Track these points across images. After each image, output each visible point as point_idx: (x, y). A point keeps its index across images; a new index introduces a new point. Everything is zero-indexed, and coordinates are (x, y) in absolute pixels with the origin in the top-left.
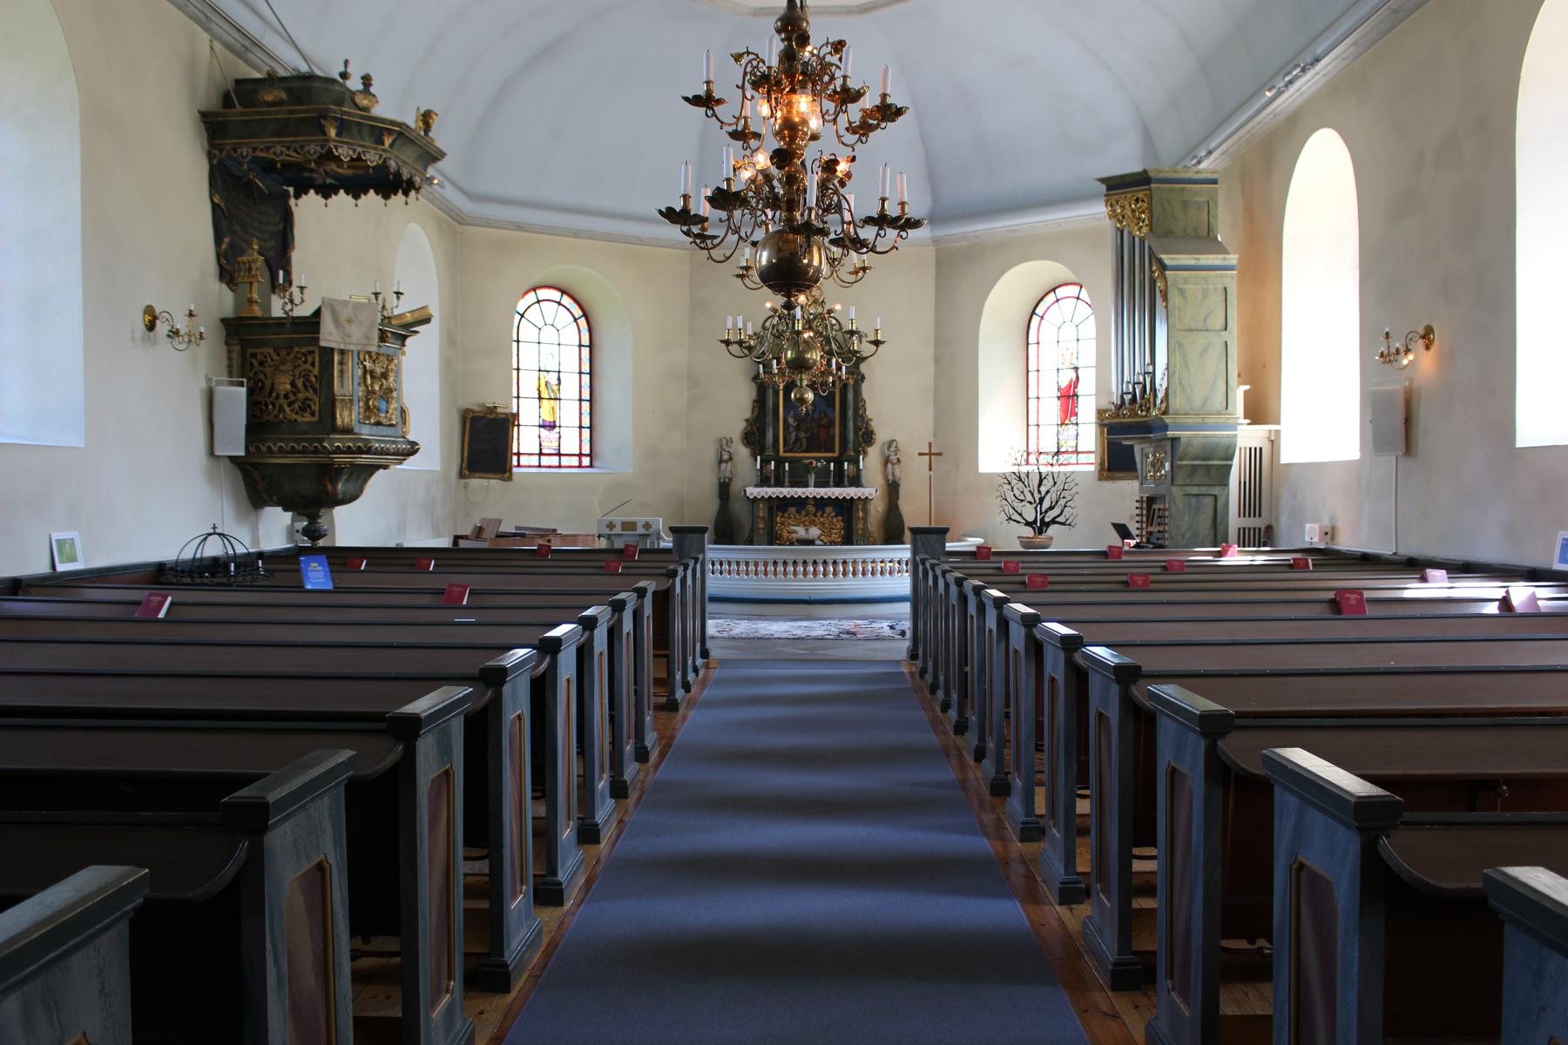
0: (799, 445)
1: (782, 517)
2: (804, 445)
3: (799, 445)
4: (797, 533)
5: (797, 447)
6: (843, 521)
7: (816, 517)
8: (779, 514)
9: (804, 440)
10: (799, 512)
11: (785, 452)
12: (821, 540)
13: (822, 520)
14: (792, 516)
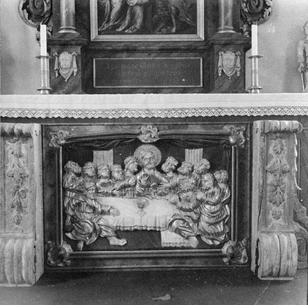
0: (128, 17)
1: (79, 175)
2: (139, 21)
3: (128, 17)
4: (118, 213)
5: (127, 22)
6: (228, 182)
7: (162, 172)
8: (73, 166)
9: (139, 11)
10: (120, 161)
11: (100, 33)
12: (178, 231)
13: (177, 179)
14: (104, 173)
